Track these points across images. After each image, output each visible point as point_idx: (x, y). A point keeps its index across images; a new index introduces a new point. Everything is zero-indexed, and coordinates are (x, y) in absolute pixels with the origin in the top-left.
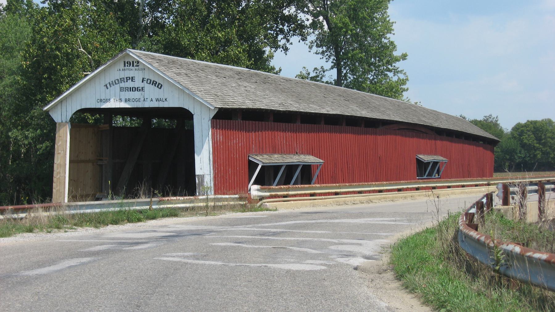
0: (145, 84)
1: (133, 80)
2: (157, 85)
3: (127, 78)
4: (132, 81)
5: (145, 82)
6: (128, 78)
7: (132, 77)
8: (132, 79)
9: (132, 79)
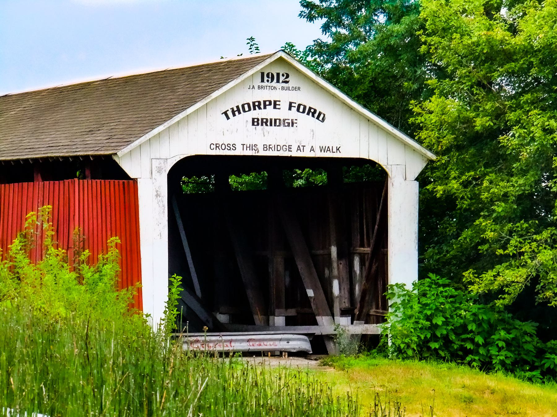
0: (293, 114)
1: (277, 107)
2: (316, 115)
3: (265, 102)
4: (275, 108)
5: (294, 109)
6: (267, 103)
7: (275, 102)
8: (275, 104)
9: (275, 104)
